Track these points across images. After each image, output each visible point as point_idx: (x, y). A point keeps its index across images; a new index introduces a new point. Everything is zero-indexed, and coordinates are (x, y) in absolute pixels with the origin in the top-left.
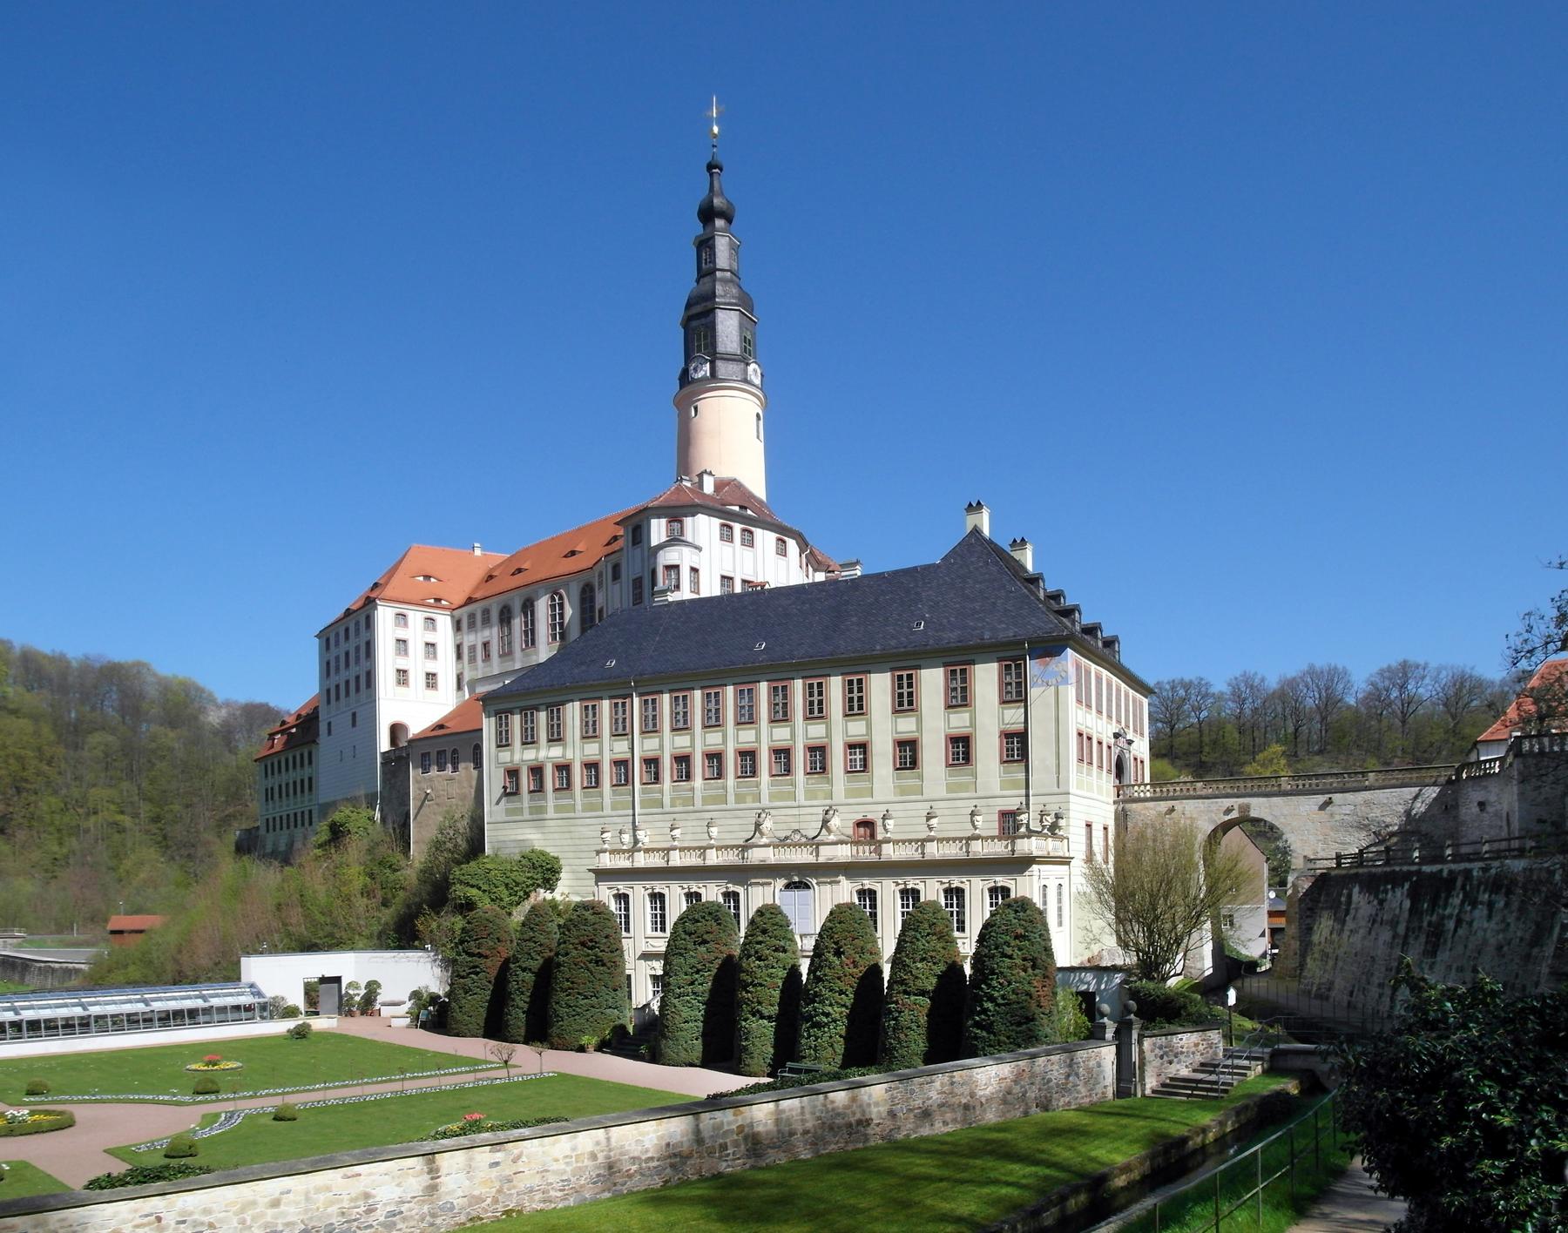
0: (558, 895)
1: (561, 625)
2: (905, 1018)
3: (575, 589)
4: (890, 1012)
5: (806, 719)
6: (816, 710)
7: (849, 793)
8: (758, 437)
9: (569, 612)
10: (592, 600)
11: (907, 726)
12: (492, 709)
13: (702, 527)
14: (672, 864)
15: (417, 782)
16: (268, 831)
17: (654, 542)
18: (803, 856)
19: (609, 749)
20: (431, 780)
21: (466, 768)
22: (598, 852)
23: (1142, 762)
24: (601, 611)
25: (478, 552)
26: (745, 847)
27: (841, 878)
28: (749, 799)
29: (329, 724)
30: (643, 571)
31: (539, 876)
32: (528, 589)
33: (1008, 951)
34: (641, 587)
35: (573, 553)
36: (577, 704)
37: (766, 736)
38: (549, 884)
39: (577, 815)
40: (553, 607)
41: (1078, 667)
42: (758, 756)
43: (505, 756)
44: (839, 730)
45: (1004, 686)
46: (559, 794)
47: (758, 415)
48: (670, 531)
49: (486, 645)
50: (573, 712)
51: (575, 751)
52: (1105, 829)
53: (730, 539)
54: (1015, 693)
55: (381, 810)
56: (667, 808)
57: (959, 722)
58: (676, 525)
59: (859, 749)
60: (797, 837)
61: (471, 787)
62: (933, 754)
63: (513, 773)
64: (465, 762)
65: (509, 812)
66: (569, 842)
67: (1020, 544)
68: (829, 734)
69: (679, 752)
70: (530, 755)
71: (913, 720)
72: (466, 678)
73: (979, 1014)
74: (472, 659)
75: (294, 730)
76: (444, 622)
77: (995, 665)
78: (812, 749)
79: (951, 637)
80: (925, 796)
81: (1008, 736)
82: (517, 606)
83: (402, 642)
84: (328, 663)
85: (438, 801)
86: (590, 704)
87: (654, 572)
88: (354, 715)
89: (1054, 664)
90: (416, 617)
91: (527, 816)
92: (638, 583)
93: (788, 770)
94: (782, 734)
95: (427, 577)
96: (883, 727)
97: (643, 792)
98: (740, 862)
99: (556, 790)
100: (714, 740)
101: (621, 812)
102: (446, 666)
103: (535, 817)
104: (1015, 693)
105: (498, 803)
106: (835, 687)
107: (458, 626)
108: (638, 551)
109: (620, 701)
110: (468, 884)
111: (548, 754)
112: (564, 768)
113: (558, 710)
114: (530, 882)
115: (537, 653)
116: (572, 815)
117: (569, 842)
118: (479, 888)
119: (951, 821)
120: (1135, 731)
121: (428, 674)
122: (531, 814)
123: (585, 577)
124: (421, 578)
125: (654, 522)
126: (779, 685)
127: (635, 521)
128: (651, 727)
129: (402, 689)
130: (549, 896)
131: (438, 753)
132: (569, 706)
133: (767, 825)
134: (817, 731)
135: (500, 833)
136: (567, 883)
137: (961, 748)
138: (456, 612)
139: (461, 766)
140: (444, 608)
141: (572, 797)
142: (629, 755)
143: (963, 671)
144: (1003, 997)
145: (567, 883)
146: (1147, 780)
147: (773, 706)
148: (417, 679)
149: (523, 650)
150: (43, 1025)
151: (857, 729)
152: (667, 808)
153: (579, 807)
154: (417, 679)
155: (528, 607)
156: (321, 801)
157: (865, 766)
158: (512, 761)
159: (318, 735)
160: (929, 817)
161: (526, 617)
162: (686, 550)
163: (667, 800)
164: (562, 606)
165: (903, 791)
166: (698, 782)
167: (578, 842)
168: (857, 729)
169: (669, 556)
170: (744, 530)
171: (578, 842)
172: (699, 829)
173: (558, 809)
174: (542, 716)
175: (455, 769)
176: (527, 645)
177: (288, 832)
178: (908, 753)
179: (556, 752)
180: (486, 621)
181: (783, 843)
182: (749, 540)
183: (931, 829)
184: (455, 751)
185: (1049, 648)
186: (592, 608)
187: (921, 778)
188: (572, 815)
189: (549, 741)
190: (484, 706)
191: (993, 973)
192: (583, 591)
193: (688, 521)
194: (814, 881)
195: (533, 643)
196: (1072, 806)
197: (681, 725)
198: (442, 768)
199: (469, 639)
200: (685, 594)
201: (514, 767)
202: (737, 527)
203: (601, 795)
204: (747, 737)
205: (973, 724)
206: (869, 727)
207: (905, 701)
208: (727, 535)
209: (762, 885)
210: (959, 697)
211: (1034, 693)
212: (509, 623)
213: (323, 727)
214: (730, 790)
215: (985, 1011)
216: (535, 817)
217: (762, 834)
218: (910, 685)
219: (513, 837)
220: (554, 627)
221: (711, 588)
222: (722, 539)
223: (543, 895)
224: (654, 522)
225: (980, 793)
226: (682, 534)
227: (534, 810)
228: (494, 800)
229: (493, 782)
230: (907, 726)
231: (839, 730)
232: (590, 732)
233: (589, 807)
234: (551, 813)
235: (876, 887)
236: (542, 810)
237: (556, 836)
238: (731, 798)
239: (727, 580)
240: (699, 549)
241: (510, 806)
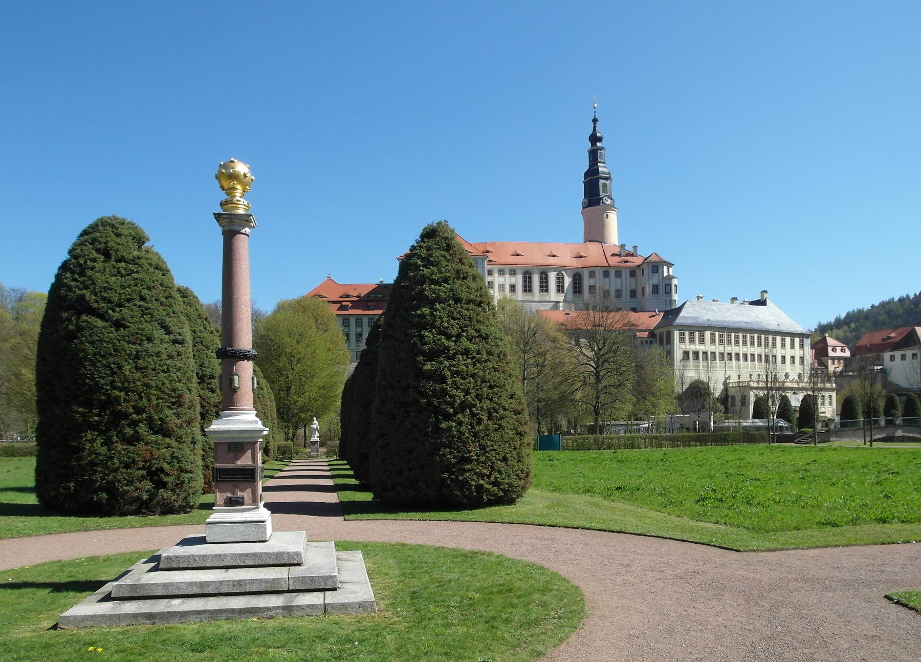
11: (783, 352)
19: (718, 349)
40: (558, 278)
43: (683, 346)
45: (800, 345)
49: (513, 288)
50: (708, 334)
51: (708, 347)
62: (788, 360)
111: (701, 348)
112: (705, 353)
115: (550, 296)
195: (547, 291)
203: (716, 363)
227: (694, 366)
229: (678, 355)
232: (713, 341)
236: (698, 366)
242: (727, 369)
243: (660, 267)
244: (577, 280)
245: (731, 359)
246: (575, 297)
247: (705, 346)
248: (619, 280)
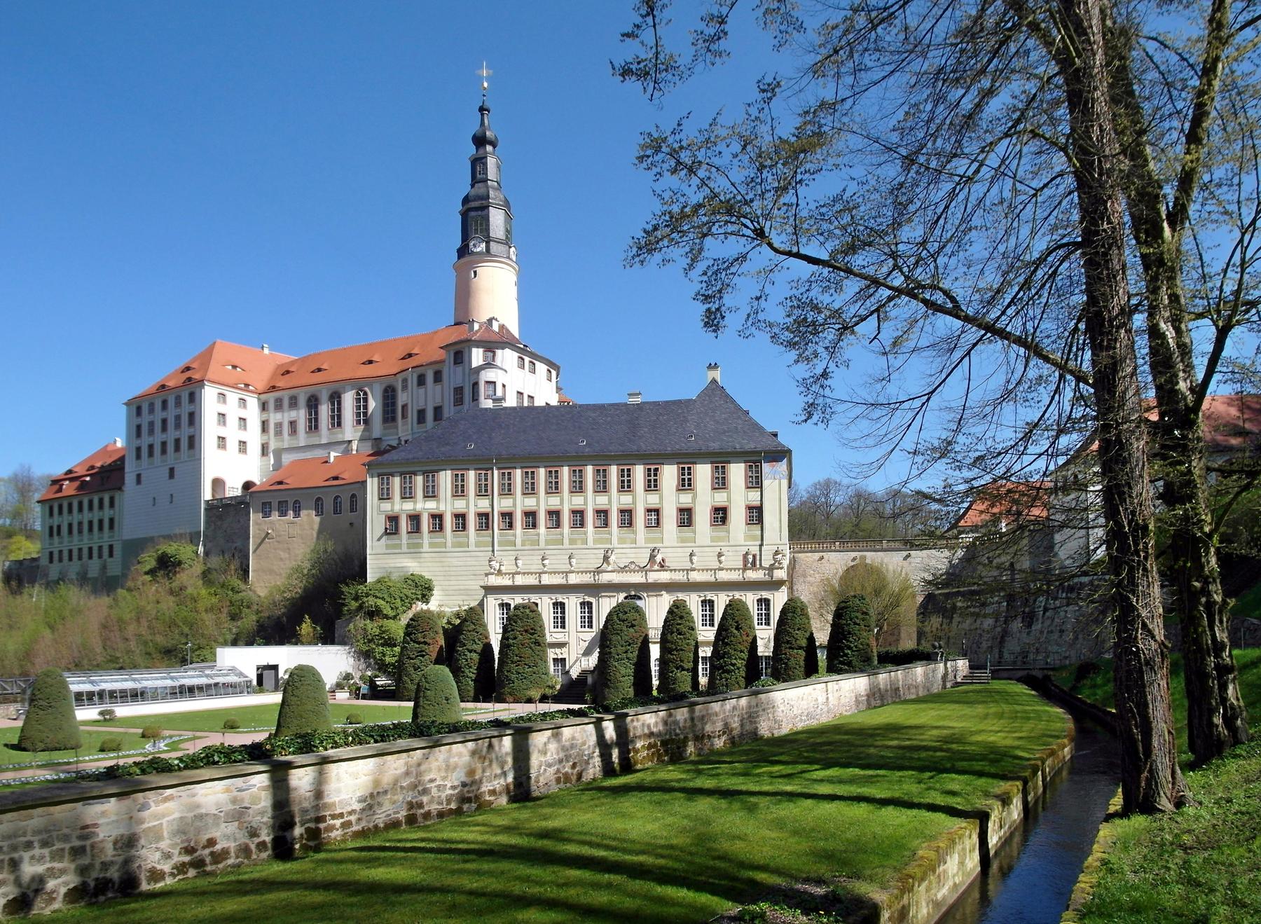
0: (433, 605)
1: (365, 414)
2: (792, 662)
3: (379, 389)
4: (782, 660)
6: (626, 485)
9: (372, 404)
10: (394, 397)
11: (686, 499)
12: (375, 472)
13: (507, 357)
14: (543, 583)
15: (256, 523)
16: (51, 561)
17: (475, 364)
18: (637, 578)
19: (473, 505)
20: (271, 522)
21: (308, 515)
22: (487, 575)
24: (404, 407)
25: (266, 351)
26: (598, 571)
27: (663, 592)
28: (579, 542)
29: (139, 476)
30: (464, 380)
31: (419, 592)
32: (337, 385)
33: (858, 621)
34: (462, 394)
35: (371, 362)
36: (449, 472)
37: (591, 501)
38: (425, 598)
39: (448, 550)
40: (358, 400)
42: (633, 513)
43: (386, 506)
44: (641, 500)
46: (433, 534)
48: (485, 358)
49: (293, 424)
50: (445, 479)
51: (447, 505)
53: (523, 367)
55: (204, 546)
56: (519, 546)
57: (720, 498)
58: (490, 354)
59: (655, 513)
60: (633, 566)
61: (313, 529)
62: (702, 517)
63: (393, 519)
64: (306, 509)
65: (387, 547)
66: (441, 569)
68: (634, 502)
69: (528, 509)
70: (408, 506)
71: (690, 495)
72: (272, 446)
73: (842, 657)
74: (278, 433)
75: (88, 479)
77: (743, 465)
78: (622, 511)
79: (715, 446)
80: (697, 544)
81: (750, 508)
82: (324, 396)
84: (139, 427)
85: (278, 539)
86: (460, 473)
87: (476, 385)
88: (172, 470)
90: (233, 397)
91: (405, 549)
92: (459, 391)
93: (606, 524)
94: (602, 501)
95: (234, 367)
96: (670, 498)
97: (501, 535)
98: (565, 582)
99: (430, 532)
100: (554, 502)
101: (482, 549)
102: (254, 436)
103: (412, 550)
104: (755, 482)
105: (379, 540)
106: (639, 472)
107: (264, 407)
108: (459, 369)
109: (483, 472)
110: (377, 597)
111: (425, 507)
112: (437, 518)
113: (433, 476)
114: (414, 597)
115: (343, 433)
116: (443, 550)
117: (441, 569)
118: (383, 599)
119: (706, 558)
121: (240, 442)
122: (408, 548)
123: (391, 381)
124: (230, 367)
125: (474, 350)
126: (601, 468)
127: (458, 347)
128: (507, 490)
129: (221, 452)
130: (425, 607)
131: (279, 502)
132: (442, 473)
133: (612, 558)
134: (626, 500)
135: (380, 561)
136: (438, 598)
137: (721, 515)
138: (264, 397)
139: (303, 513)
140: (252, 392)
141: (445, 537)
142: (490, 510)
143: (723, 467)
144: (856, 647)
145: (438, 598)
147: (596, 482)
148: (232, 445)
149: (329, 429)
150: (85, 698)
151: (653, 500)
152: (517, 548)
153: (449, 544)
154: (232, 445)
155: (336, 398)
156: (125, 538)
157: (658, 523)
158: (392, 510)
159: (123, 483)
160: (720, 555)
161: (333, 404)
162: (500, 371)
163: (519, 541)
164: (366, 400)
165: (683, 540)
167: (447, 569)
168: (653, 500)
169: (488, 375)
171: (447, 569)
172: (536, 562)
173: (431, 545)
174: (419, 480)
175: (297, 515)
176: (333, 425)
177: (79, 562)
178: (686, 517)
179: (431, 505)
180: (293, 403)
181: (623, 570)
183: (720, 562)
184: (296, 502)
186: (394, 404)
187: (695, 532)
188: (443, 550)
189: (425, 497)
190: (368, 470)
191: (849, 633)
192: (386, 391)
193: (499, 352)
194: (645, 595)
195: (339, 424)
197: (530, 489)
198: (283, 513)
199: (274, 417)
201: (395, 515)
203: (468, 537)
204: (578, 501)
205: (729, 500)
206: (661, 498)
207: (686, 484)
209: (609, 597)
210: (720, 483)
211: (766, 483)
212: (316, 407)
213: (129, 478)
214: (566, 535)
215: (846, 655)
216: (412, 550)
217: (609, 564)
218: (629, 476)
219: (392, 565)
220: (358, 415)
223: (420, 606)
224: (474, 350)
226: (494, 360)
228: (376, 538)
229: (375, 525)
230: (686, 499)
231: (641, 500)
232: (459, 490)
233: (460, 545)
234: (426, 547)
236: (420, 545)
237: (429, 564)
238: (566, 541)
241: (389, 542)
242: (496, 547)
243: (467, 350)
244: (389, 396)
245: (511, 526)
246: (385, 429)
247: (438, 501)
248: (438, 387)
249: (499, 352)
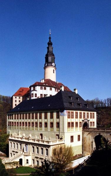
5: (35, 119)
7: (40, 130)
8: (54, 73)
13: (38, 88)
17: (32, 90)
19: (17, 121)
23: (94, 122)
26: (22, 138)
41: (69, 112)
47: (54, 70)
52: (79, 136)
54: (58, 117)
59: (41, 123)
63: (9, 122)
67: (75, 90)
76: (21, 98)
83: (16, 101)
89: (63, 113)
90: (18, 97)
96: (43, 121)
104: (58, 117)
120: (91, 118)
134: (36, 120)
146: (95, 127)
151: (41, 120)
157: (41, 126)
166: (25, 126)
170: (44, 88)
182: (45, 89)
185: (62, 111)
187: (47, 128)
196: (65, 135)
200: (34, 98)
202: (43, 87)
205: (53, 121)
206: (42, 120)
208: (42, 89)
211: (60, 117)
221: (39, 96)
222: (41, 89)
225: (54, 131)
231: (39, 121)
234: (12, 129)
235: (34, 146)
239: (41, 95)
240: (37, 91)
249: (36, 87)
